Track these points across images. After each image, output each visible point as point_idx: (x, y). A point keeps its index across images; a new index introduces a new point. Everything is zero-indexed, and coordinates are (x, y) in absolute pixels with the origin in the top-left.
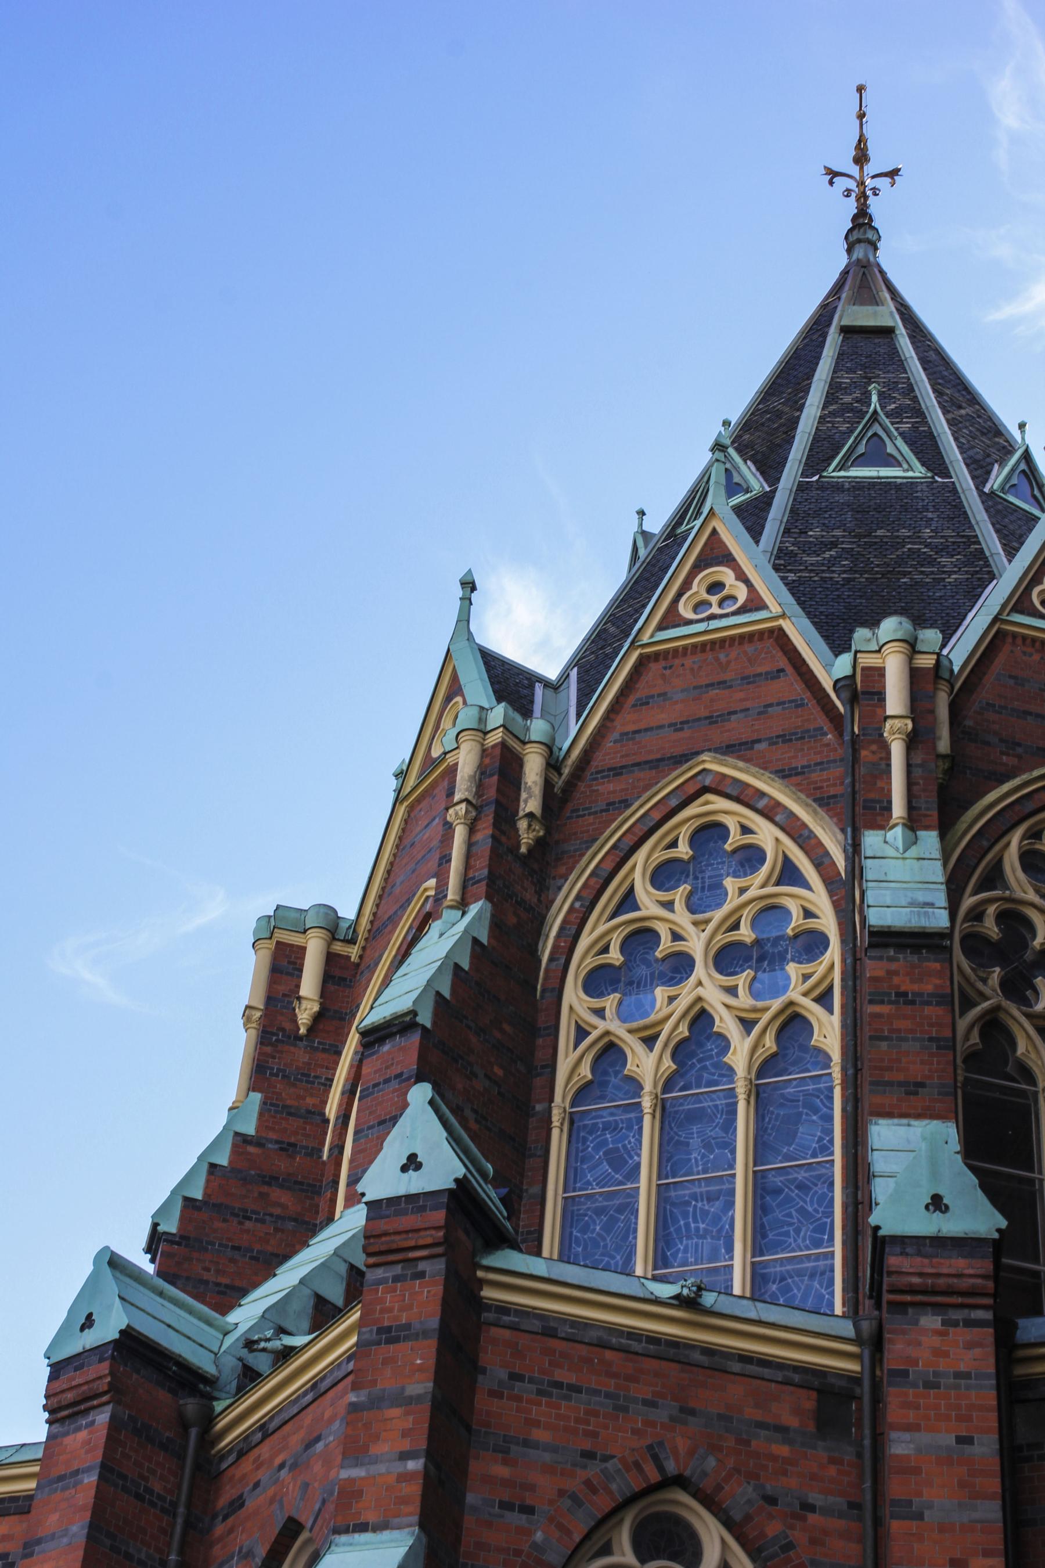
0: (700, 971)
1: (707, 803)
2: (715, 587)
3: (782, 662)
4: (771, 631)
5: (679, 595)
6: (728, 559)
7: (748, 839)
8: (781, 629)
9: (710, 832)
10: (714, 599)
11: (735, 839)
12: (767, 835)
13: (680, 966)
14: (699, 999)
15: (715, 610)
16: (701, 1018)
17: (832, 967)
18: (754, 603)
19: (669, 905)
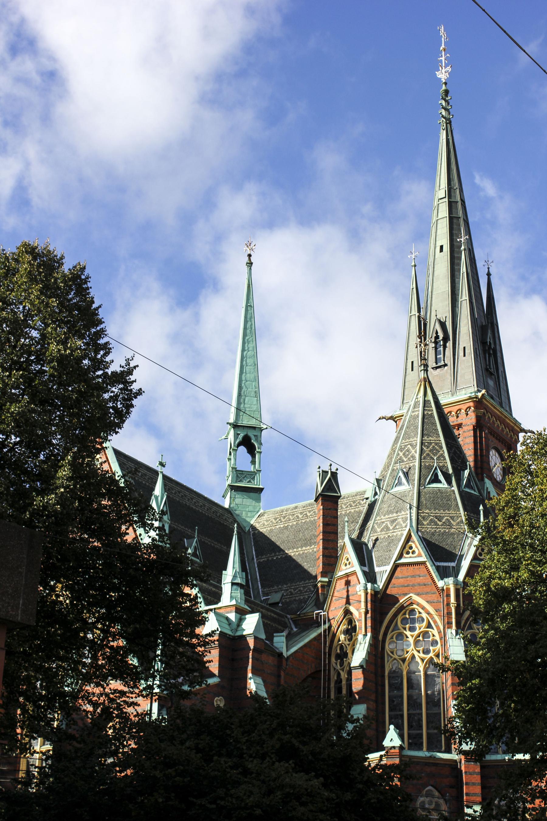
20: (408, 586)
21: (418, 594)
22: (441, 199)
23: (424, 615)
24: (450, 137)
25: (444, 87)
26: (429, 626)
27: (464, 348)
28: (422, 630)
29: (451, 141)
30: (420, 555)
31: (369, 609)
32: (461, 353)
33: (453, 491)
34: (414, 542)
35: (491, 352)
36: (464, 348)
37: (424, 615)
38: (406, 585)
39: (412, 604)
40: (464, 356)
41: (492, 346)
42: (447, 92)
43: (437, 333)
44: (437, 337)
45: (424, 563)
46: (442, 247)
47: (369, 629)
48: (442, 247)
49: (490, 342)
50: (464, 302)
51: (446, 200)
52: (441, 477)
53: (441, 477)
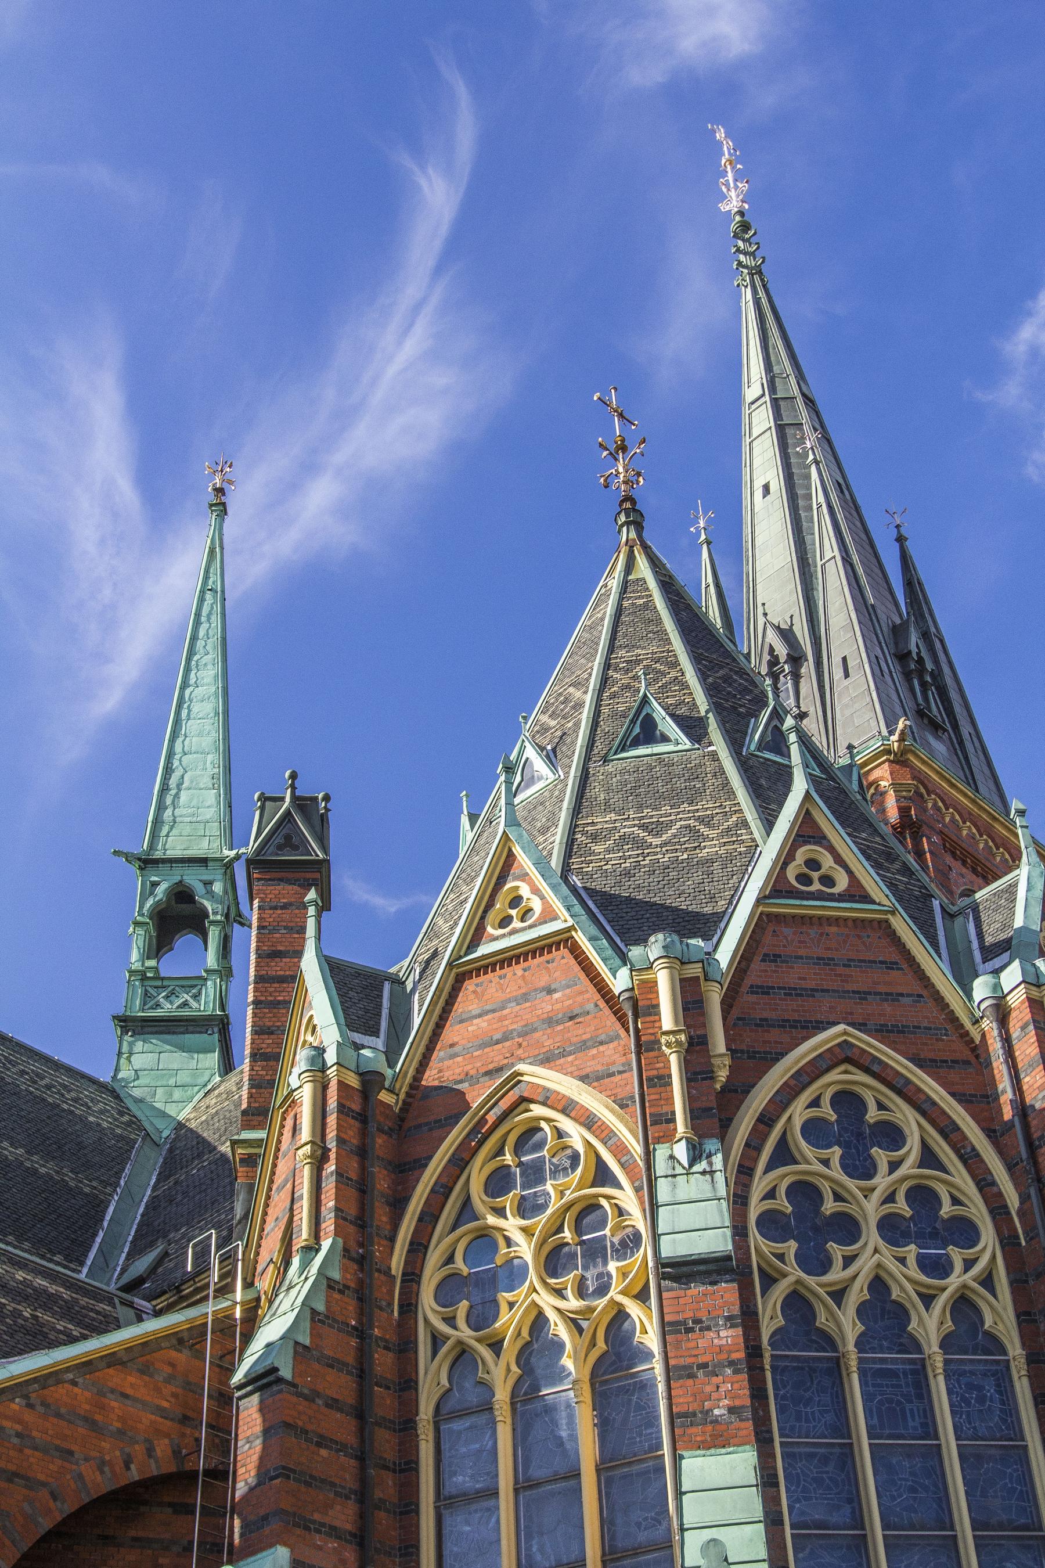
0: (872, 1236)
1: (846, 1072)
2: (813, 864)
3: (895, 957)
4: (879, 922)
5: (785, 864)
6: (820, 839)
7: (884, 1115)
8: (887, 921)
9: (847, 1101)
10: (815, 875)
11: (872, 1115)
12: (908, 1118)
13: (847, 1228)
14: (879, 1265)
15: (816, 886)
16: (879, 1285)
17: (994, 1257)
18: (857, 893)
19: (826, 1162)
20: (505, 1038)
21: (547, 1060)
22: (753, 403)
23: (577, 1136)
24: (761, 294)
25: (738, 218)
26: (602, 1175)
27: (844, 659)
28: (569, 1196)
29: (764, 301)
30: (549, 915)
31: (332, 1145)
32: (838, 673)
33: (714, 757)
34: (524, 877)
35: (929, 679)
36: (844, 659)
37: (577, 1136)
38: (497, 1036)
39: (524, 1100)
40: (847, 675)
41: (929, 666)
42: (745, 226)
43: (772, 650)
44: (774, 661)
45: (563, 940)
46: (766, 489)
47: (329, 1225)
48: (766, 489)
49: (919, 654)
50: (831, 567)
51: (767, 398)
52: (667, 725)
53: (667, 725)
